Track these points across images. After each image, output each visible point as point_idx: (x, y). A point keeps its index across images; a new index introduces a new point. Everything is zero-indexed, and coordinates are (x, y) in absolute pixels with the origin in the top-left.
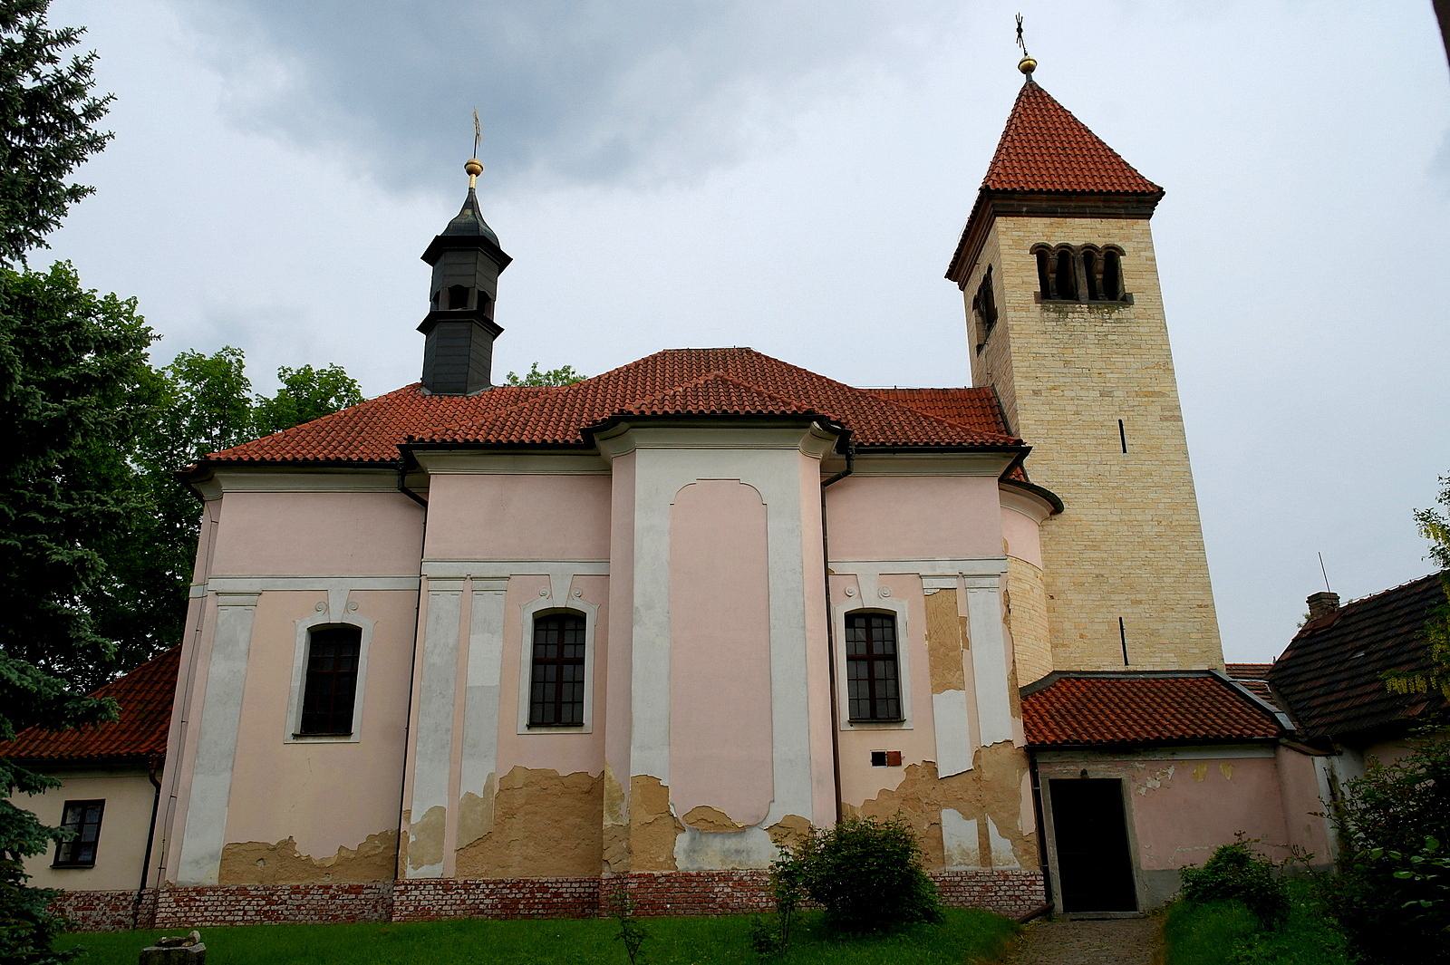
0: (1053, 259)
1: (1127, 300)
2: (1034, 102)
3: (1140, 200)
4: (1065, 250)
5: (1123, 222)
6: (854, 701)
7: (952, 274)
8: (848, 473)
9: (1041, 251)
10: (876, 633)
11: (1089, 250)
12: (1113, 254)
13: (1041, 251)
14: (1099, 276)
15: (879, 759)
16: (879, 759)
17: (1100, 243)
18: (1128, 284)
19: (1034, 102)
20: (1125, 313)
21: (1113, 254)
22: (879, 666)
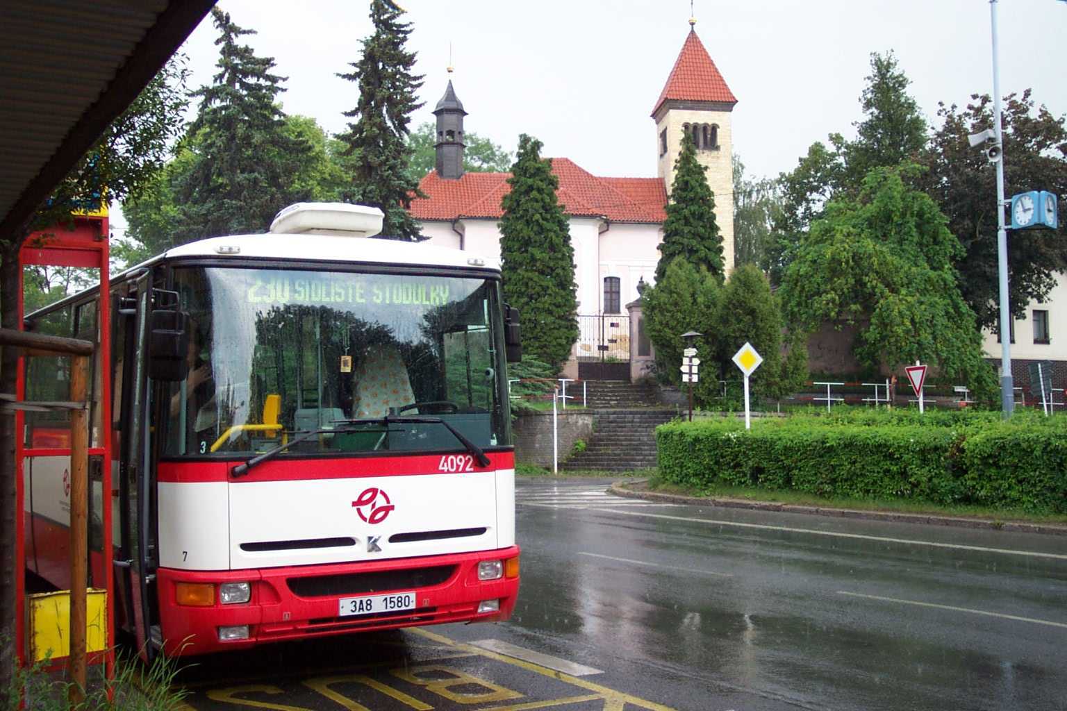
0: (691, 129)
1: (717, 148)
2: (693, 39)
3: (728, 104)
4: (696, 126)
5: (721, 113)
6: (606, 306)
7: (654, 115)
8: (607, 230)
9: (686, 126)
10: (614, 284)
11: (705, 127)
12: (714, 128)
13: (686, 126)
14: (709, 136)
15: (612, 325)
16: (612, 325)
17: (710, 123)
18: (719, 141)
19: (693, 39)
20: (715, 153)
21: (714, 128)
22: (614, 296)
